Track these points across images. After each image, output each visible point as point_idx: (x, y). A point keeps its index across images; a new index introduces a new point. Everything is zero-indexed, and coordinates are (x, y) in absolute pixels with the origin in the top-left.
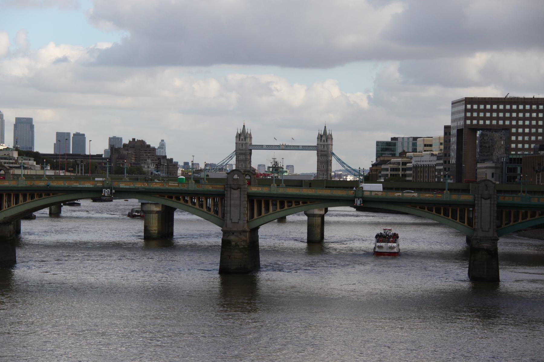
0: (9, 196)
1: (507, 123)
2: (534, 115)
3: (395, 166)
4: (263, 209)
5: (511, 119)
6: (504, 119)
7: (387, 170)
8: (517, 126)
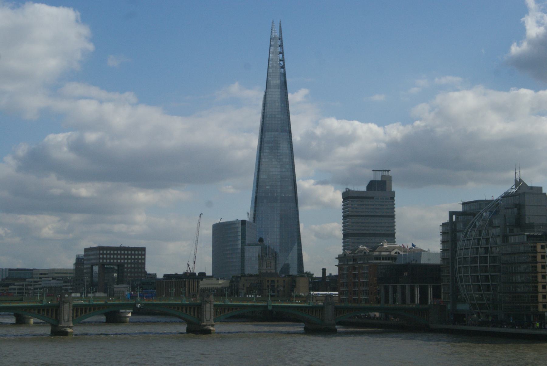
0: (190, 308)
1: (122, 261)
2: (115, 256)
3: (21, 287)
4: (79, 314)
5: (124, 259)
6: (121, 259)
7: (15, 289)
8: (128, 263)
